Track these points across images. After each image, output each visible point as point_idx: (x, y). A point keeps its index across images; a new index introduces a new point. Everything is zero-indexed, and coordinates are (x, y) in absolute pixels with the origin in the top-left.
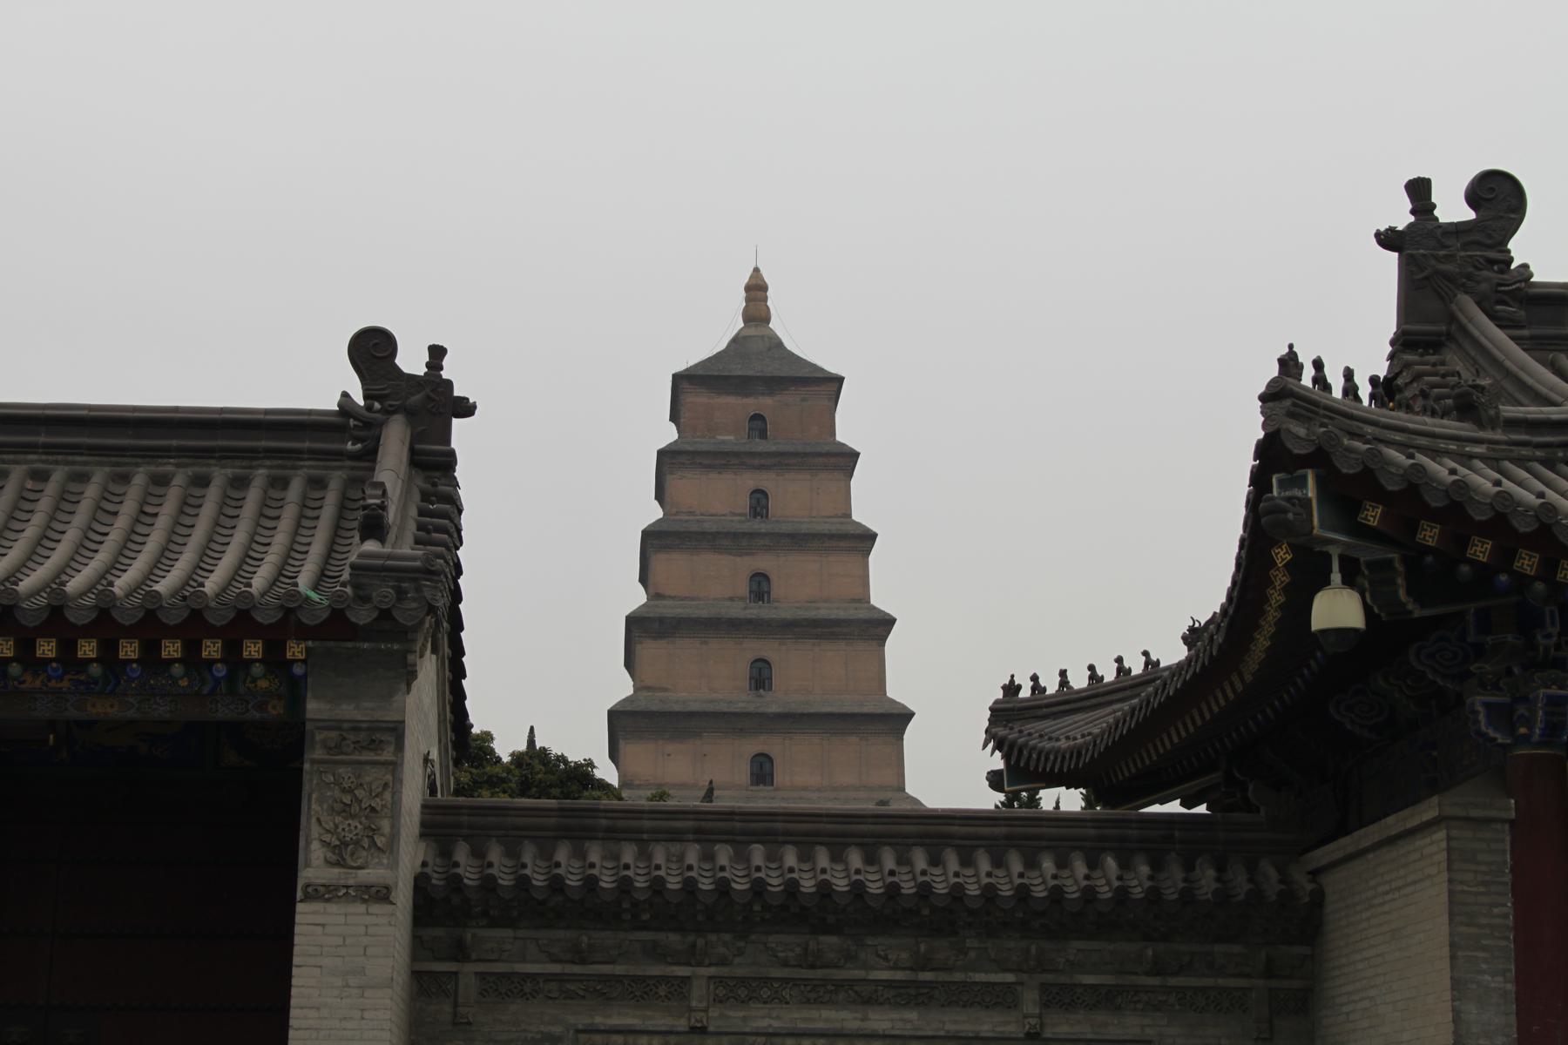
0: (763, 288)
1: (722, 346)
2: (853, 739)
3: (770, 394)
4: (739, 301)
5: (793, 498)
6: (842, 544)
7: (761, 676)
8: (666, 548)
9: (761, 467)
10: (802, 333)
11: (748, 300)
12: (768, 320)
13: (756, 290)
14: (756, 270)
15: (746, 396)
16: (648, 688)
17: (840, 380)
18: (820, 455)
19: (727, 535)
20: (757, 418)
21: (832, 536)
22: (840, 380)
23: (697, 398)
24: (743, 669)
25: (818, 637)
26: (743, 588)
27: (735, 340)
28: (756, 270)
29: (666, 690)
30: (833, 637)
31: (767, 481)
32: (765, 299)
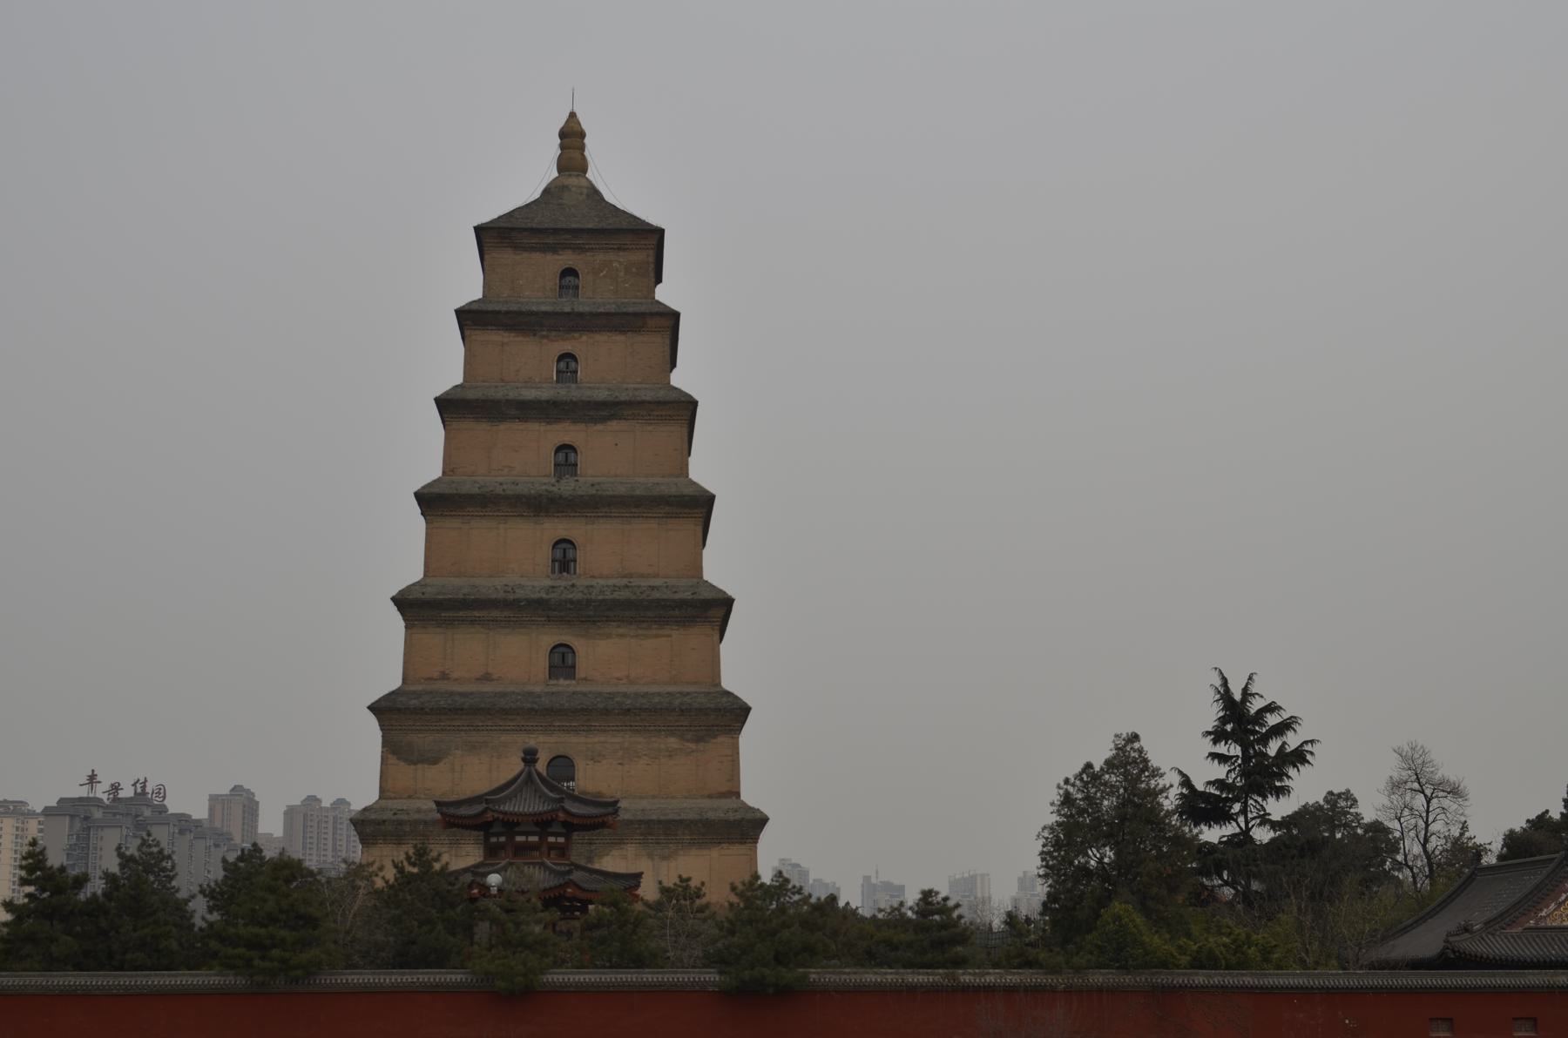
0: (582, 135)
1: (537, 195)
4: (551, 148)
5: (605, 363)
7: (564, 557)
10: (621, 182)
11: (562, 147)
12: (585, 170)
13: (572, 137)
14: (572, 115)
20: (569, 272)
24: (544, 555)
27: (546, 191)
28: (572, 115)
31: (577, 344)
32: (582, 148)
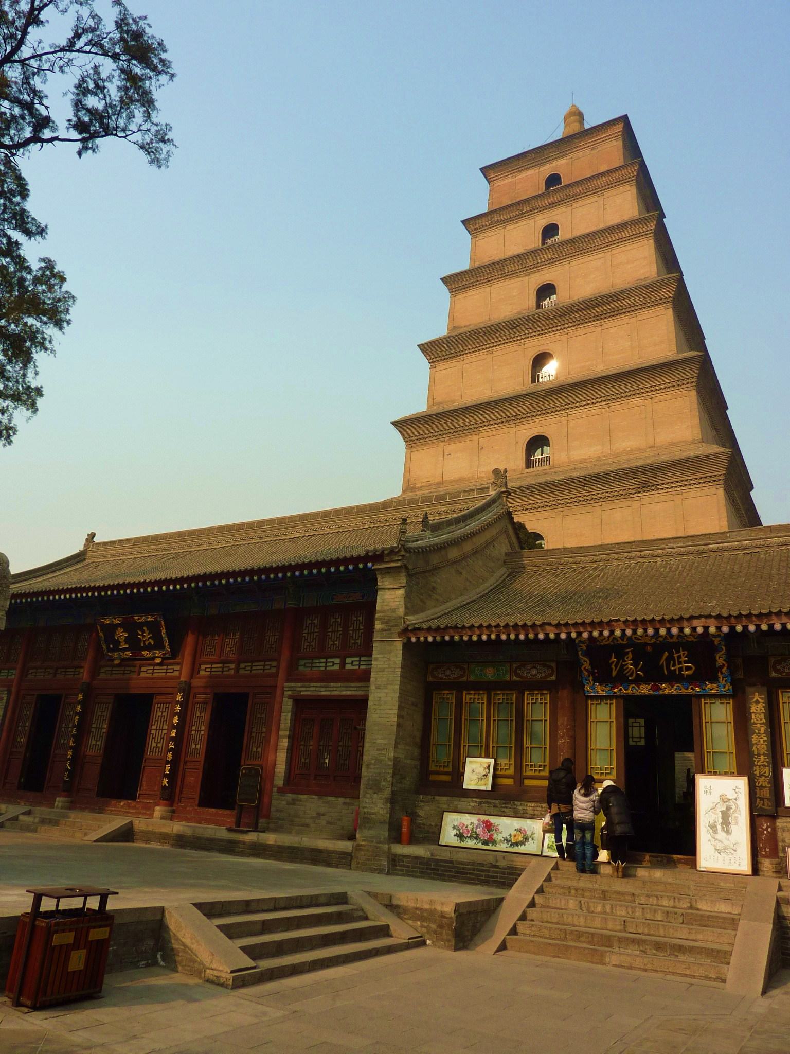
2: (637, 401)
3: (564, 154)
6: (625, 234)
8: (465, 288)
9: (552, 205)
15: (542, 164)
16: (439, 404)
17: (625, 119)
18: (601, 175)
19: (512, 259)
21: (611, 230)
22: (625, 119)
23: (505, 181)
25: (599, 317)
26: (532, 301)
29: (453, 402)
30: (615, 313)
